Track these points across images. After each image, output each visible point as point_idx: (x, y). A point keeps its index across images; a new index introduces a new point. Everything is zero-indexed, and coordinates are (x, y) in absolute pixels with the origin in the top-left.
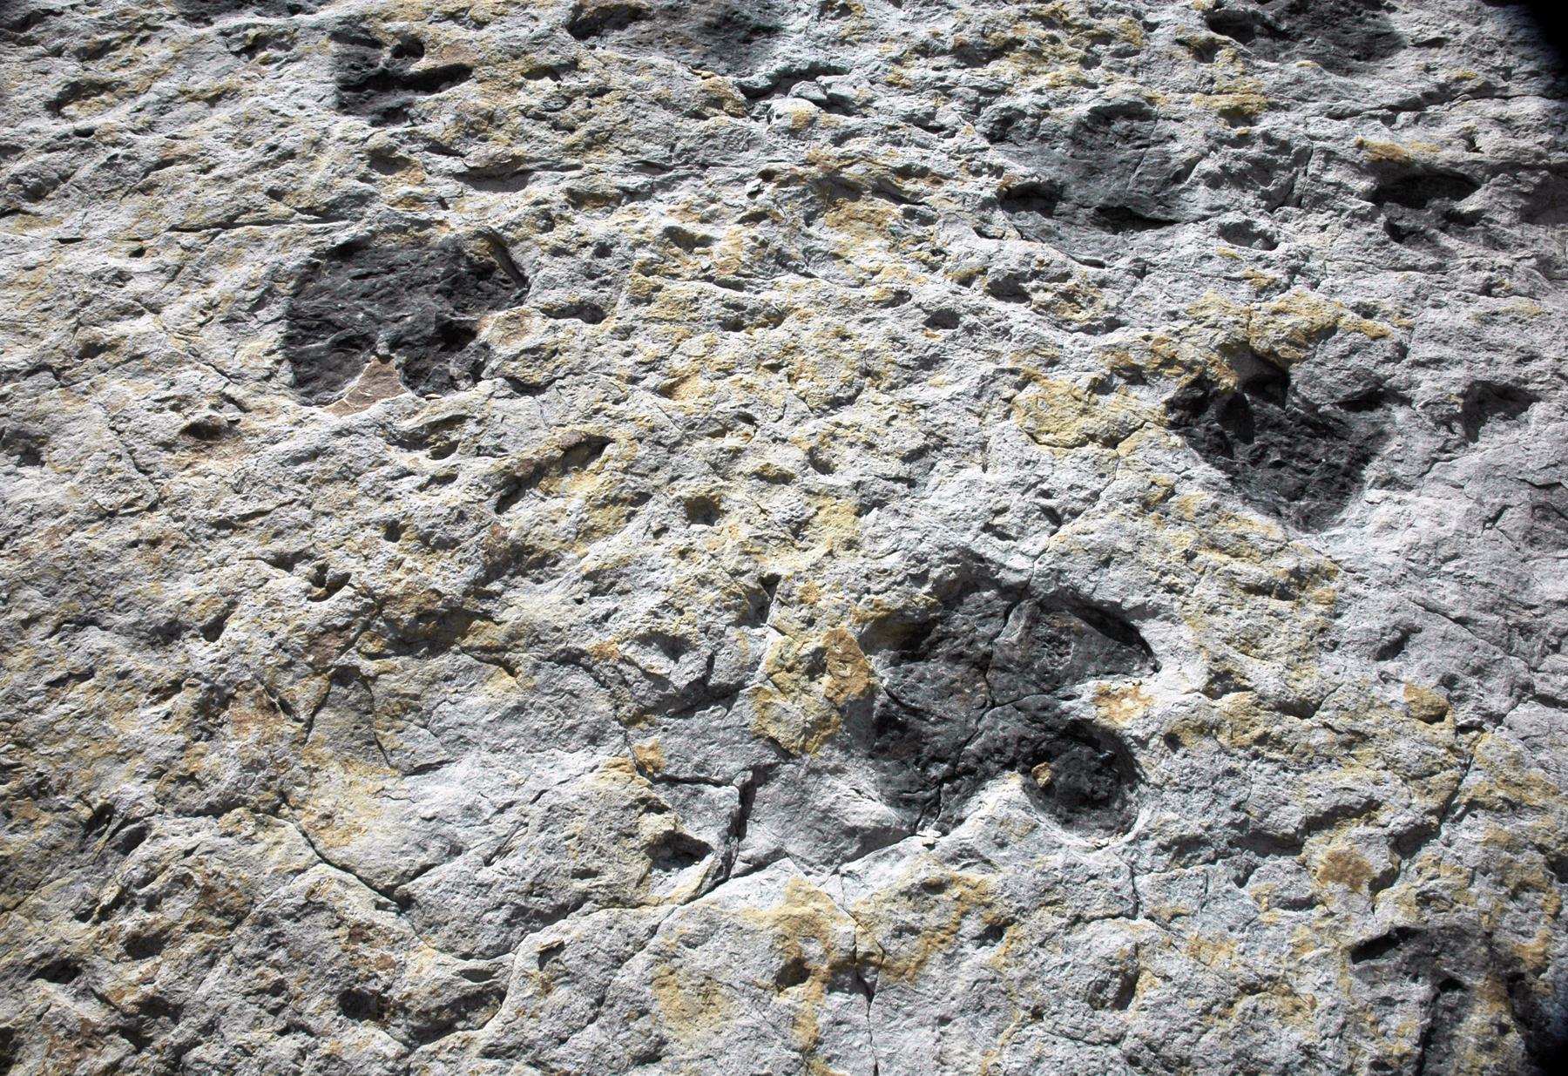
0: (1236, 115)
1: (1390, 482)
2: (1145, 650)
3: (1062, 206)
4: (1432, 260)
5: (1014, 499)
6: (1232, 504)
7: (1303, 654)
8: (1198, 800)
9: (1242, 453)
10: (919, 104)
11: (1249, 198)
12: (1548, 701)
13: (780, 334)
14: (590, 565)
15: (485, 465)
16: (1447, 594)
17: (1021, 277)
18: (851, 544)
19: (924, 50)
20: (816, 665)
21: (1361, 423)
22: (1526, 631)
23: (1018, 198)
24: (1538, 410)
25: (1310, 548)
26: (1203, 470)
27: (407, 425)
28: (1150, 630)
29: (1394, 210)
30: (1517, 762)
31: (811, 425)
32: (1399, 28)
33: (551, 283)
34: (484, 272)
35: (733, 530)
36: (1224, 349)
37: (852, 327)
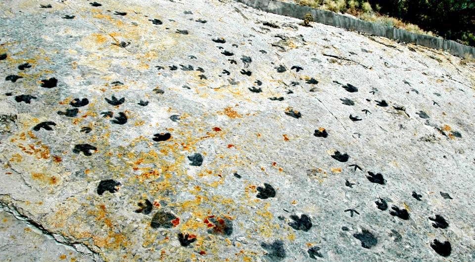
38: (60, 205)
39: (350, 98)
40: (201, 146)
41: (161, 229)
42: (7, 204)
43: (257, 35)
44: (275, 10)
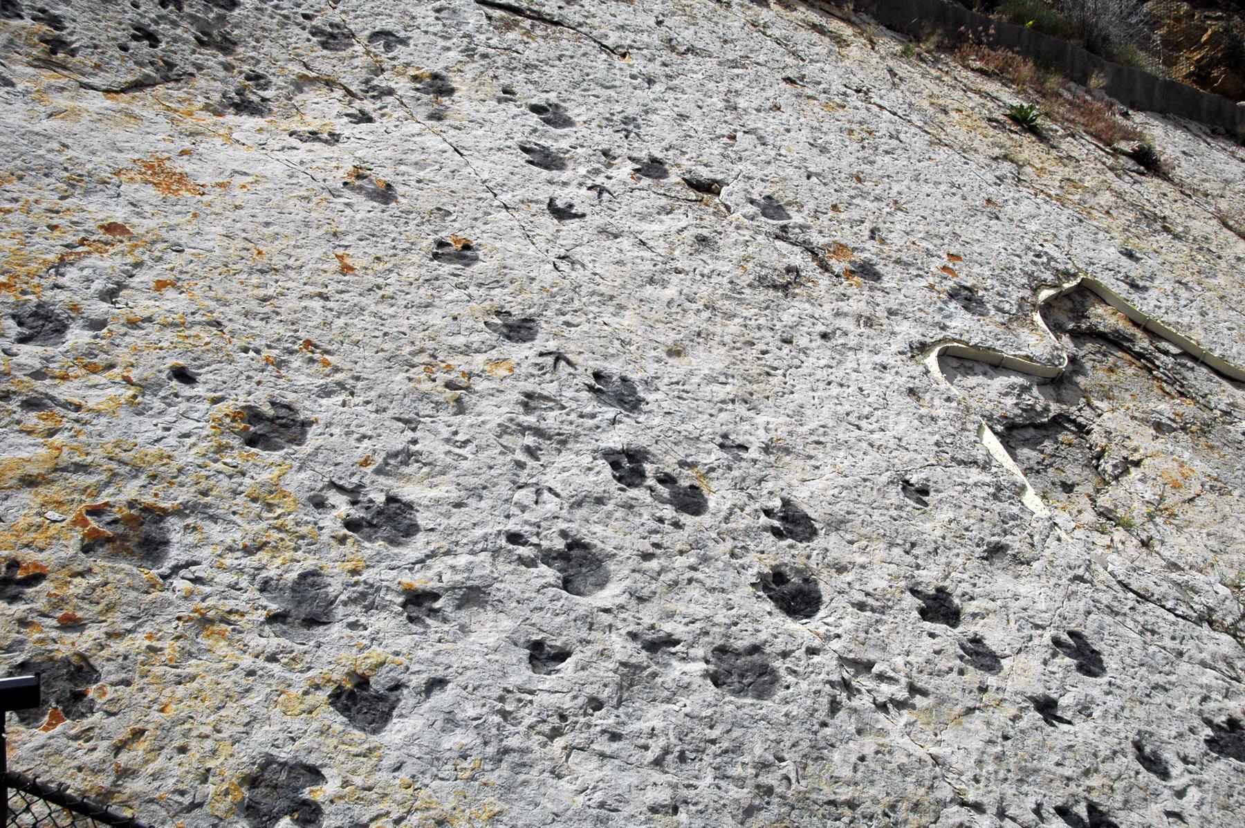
0: (354, 572)
1: (401, 716)
2: (323, 777)
3: (289, 620)
4: (422, 630)
5: (281, 735)
6: (350, 729)
7: (370, 773)
8: (340, 817)
9: (354, 710)
11: (358, 609)
12: (442, 779)
13: (195, 685)
14: (150, 771)
15: (106, 743)
16: (415, 750)
17: (276, 653)
18: (232, 755)
19: (231, 549)
20: (227, 793)
21: (392, 696)
22: (438, 759)
23: (273, 619)
24: (450, 686)
25: (374, 740)
26: (341, 718)
27: (73, 732)
28: (324, 771)
29: (411, 607)
30: (430, 797)
31: (212, 718)
33: (109, 673)
34: (79, 669)
35: (194, 756)
36: (348, 674)
37: (220, 680)
39: (553, 145)
40: (61, 281)
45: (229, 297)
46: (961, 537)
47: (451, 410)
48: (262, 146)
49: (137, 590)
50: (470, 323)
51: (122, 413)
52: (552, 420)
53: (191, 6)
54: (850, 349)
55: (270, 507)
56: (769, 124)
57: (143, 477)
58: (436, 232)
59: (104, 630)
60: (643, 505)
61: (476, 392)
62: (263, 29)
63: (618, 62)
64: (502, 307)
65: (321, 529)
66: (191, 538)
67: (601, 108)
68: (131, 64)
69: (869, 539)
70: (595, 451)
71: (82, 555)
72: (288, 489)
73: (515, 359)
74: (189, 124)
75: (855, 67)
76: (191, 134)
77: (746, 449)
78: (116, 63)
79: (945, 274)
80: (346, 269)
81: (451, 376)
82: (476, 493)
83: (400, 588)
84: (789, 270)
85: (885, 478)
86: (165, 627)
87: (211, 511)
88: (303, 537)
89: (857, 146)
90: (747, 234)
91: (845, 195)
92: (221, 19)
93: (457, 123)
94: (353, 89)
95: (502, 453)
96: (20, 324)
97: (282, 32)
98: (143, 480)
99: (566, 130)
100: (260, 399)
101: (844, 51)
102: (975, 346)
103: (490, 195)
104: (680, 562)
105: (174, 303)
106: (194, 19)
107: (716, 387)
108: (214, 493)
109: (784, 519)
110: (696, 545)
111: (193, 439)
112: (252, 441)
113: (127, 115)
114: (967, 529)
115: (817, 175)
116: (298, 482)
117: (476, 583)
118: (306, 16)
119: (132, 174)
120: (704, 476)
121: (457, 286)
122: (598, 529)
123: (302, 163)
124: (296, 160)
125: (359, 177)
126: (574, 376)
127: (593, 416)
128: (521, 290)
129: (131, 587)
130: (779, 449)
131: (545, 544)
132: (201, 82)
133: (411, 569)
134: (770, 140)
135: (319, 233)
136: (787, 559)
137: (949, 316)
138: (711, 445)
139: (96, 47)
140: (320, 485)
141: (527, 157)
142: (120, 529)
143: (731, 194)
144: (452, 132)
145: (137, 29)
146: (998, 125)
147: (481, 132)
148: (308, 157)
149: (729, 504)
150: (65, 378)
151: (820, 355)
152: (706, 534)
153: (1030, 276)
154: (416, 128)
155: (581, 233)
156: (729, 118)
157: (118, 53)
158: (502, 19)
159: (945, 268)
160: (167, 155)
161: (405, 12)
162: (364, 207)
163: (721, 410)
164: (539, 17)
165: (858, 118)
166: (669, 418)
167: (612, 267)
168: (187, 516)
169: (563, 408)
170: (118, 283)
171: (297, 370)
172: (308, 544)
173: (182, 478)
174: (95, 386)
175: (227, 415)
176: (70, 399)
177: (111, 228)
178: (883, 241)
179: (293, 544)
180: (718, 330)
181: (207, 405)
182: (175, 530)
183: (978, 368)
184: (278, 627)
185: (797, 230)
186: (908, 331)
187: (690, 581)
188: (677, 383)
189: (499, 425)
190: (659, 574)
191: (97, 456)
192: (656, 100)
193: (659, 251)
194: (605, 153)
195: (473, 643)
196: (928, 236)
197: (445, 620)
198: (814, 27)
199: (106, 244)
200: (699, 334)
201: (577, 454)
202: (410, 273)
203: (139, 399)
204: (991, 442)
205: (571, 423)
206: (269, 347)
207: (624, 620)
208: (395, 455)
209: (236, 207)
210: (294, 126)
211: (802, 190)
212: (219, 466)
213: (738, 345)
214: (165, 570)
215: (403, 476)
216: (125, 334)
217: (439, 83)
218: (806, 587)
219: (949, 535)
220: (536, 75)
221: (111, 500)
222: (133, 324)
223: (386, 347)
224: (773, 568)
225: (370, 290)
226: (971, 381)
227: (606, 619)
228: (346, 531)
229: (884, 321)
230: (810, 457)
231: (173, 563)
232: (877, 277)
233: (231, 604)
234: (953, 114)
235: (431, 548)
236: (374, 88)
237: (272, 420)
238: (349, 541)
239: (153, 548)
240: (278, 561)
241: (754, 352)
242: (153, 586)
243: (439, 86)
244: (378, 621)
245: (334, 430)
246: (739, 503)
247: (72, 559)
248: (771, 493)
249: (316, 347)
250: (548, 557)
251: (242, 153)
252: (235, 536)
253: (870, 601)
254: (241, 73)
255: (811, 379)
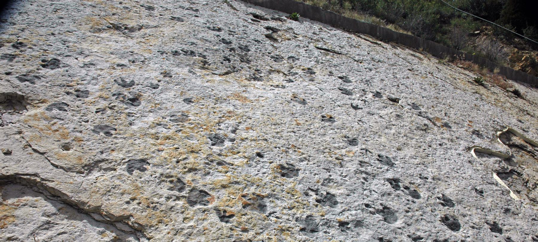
0: (322, 216)
3: (306, 230)
10: (287, 217)
19: (284, 208)
23: (302, 230)
32: (339, 201)
38: (92, 184)
40: (220, 127)
41: (198, 206)
42: (36, 184)
43: (250, 26)
44: (263, 3)
45: (267, 132)
46: (496, 206)
47: (339, 166)
48: (265, 89)
49: (260, 220)
50: (338, 140)
51: (245, 166)
52: (369, 169)
53: (238, 51)
54: (449, 149)
55: (293, 195)
56: (408, 82)
57: (255, 186)
58: (321, 113)
59: (254, 232)
60: (402, 196)
61: (345, 161)
62: (258, 57)
63: (361, 65)
64: (346, 135)
65: (309, 202)
66: (272, 205)
67: (359, 77)
68: (224, 67)
69: (470, 206)
70: (384, 179)
71: (243, 209)
72: (298, 190)
73: (354, 150)
74: (243, 83)
75: (427, 66)
76: (244, 86)
77: (427, 179)
78: (221, 67)
79: (470, 127)
80: (298, 124)
81: (337, 156)
82: (353, 191)
83: (337, 221)
84: (425, 125)
85: (470, 188)
86: (271, 232)
87: (276, 196)
88: (305, 205)
89: (434, 89)
90: (410, 114)
91: (435, 103)
92: (246, 54)
93: (318, 82)
94: (286, 73)
95: (357, 179)
96: (211, 140)
97: (263, 58)
98: (255, 187)
99: (350, 84)
100: (283, 162)
101: (423, 62)
102: (484, 148)
103: (334, 102)
104: (417, 213)
105: (252, 134)
106: (239, 55)
107: (414, 160)
108: (276, 191)
109: (444, 200)
110: (421, 208)
111: (267, 174)
112: (283, 175)
113: (226, 81)
114: (497, 204)
115: (425, 97)
116: (299, 187)
117: (359, 219)
118: (269, 53)
119: (232, 97)
120: (417, 187)
121: (331, 129)
122: (391, 203)
123: (277, 93)
124: (276, 92)
125: (295, 97)
126: (373, 156)
127: (381, 168)
128: (350, 130)
129: (259, 219)
130: (437, 179)
131: (376, 207)
132: (243, 72)
133: (339, 215)
134: (409, 87)
135: (288, 113)
136: (448, 213)
137: (474, 139)
138: (417, 178)
139: (215, 63)
140: (306, 189)
141: (341, 91)
142: (252, 201)
143: (402, 102)
144: (318, 85)
145: (225, 58)
146: (472, 83)
147: (326, 84)
148: (279, 92)
149: (427, 196)
150: (226, 156)
151: (440, 151)
152: (422, 205)
153: (493, 127)
154: (307, 84)
155: (363, 113)
156: (396, 80)
157: (221, 65)
158: (324, 53)
159: (469, 125)
160: (239, 92)
161: (296, 51)
162: (299, 106)
163: (417, 167)
164: (334, 52)
165: (432, 81)
166: (403, 169)
167: (375, 124)
168: (270, 198)
169: (372, 166)
170: (235, 128)
171: (291, 154)
172: (307, 207)
173: (266, 186)
174: (235, 158)
175: (275, 167)
176: (230, 162)
177: (230, 112)
178: (449, 117)
179: (302, 207)
180: (410, 142)
181: (268, 164)
182: (267, 202)
183: (485, 155)
184: (304, 232)
185: (424, 113)
186: (463, 144)
187: (422, 219)
188: (402, 158)
189: (354, 171)
190: (412, 217)
191: (240, 179)
192: (374, 75)
193: (387, 119)
194: (363, 90)
195: (362, 238)
196: (461, 115)
197: (352, 231)
198: (412, 55)
199: (230, 117)
200: (405, 144)
201: (379, 180)
202: (317, 125)
203: (249, 162)
204: (495, 176)
205: (375, 170)
206: (282, 147)
207: (405, 231)
208: (326, 180)
209: (263, 106)
210: (271, 84)
211: (422, 101)
212: (276, 182)
213: (416, 147)
214: (267, 214)
215: (329, 186)
216: (241, 143)
217: (310, 71)
218: (455, 221)
219: (493, 206)
220: (338, 68)
221: (248, 192)
222: (242, 140)
223: (316, 147)
224: (445, 215)
225: (307, 130)
226: (484, 159)
227: (400, 231)
228: (317, 203)
229: (456, 140)
230: (446, 181)
231: (269, 212)
232: (450, 127)
233: (288, 225)
234: (458, 80)
235: (343, 208)
236: (292, 73)
237: (288, 169)
238: (319, 206)
239: (262, 207)
240: (299, 212)
241: (421, 150)
242: (265, 219)
243: (310, 71)
244: (332, 231)
245: (307, 172)
246: (430, 195)
247: (241, 210)
248: (438, 192)
249: (296, 147)
250: (378, 211)
251: (260, 91)
252: (284, 204)
253: (475, 226)
254: (253, 69)
255: (440, 157)
